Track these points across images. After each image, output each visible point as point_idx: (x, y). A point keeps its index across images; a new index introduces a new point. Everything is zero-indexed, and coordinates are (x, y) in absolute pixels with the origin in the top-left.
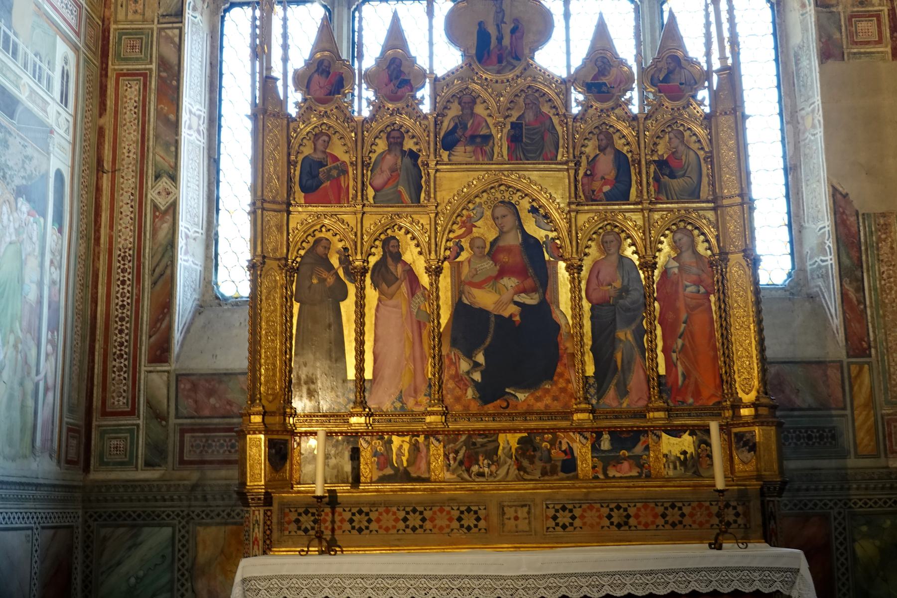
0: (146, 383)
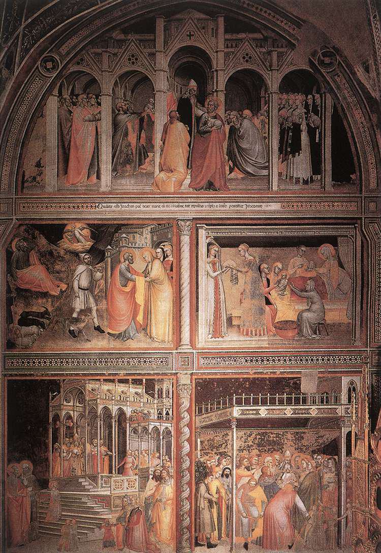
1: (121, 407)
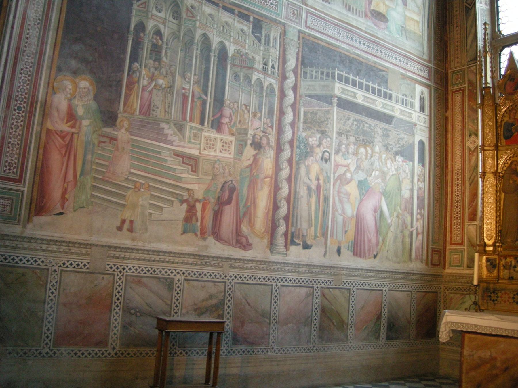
0: (467, 230)
1: (224, 41)
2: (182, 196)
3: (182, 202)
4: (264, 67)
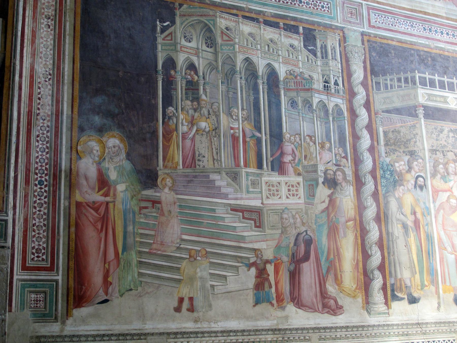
2: (248, 258)
3: (250, 266)
4: (325, 85)
